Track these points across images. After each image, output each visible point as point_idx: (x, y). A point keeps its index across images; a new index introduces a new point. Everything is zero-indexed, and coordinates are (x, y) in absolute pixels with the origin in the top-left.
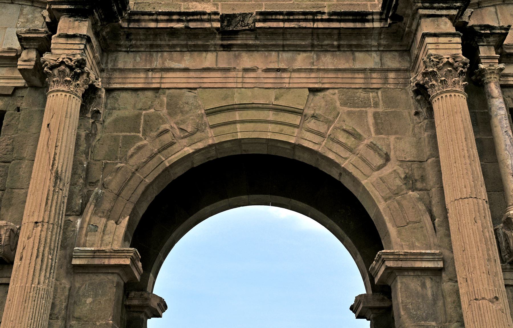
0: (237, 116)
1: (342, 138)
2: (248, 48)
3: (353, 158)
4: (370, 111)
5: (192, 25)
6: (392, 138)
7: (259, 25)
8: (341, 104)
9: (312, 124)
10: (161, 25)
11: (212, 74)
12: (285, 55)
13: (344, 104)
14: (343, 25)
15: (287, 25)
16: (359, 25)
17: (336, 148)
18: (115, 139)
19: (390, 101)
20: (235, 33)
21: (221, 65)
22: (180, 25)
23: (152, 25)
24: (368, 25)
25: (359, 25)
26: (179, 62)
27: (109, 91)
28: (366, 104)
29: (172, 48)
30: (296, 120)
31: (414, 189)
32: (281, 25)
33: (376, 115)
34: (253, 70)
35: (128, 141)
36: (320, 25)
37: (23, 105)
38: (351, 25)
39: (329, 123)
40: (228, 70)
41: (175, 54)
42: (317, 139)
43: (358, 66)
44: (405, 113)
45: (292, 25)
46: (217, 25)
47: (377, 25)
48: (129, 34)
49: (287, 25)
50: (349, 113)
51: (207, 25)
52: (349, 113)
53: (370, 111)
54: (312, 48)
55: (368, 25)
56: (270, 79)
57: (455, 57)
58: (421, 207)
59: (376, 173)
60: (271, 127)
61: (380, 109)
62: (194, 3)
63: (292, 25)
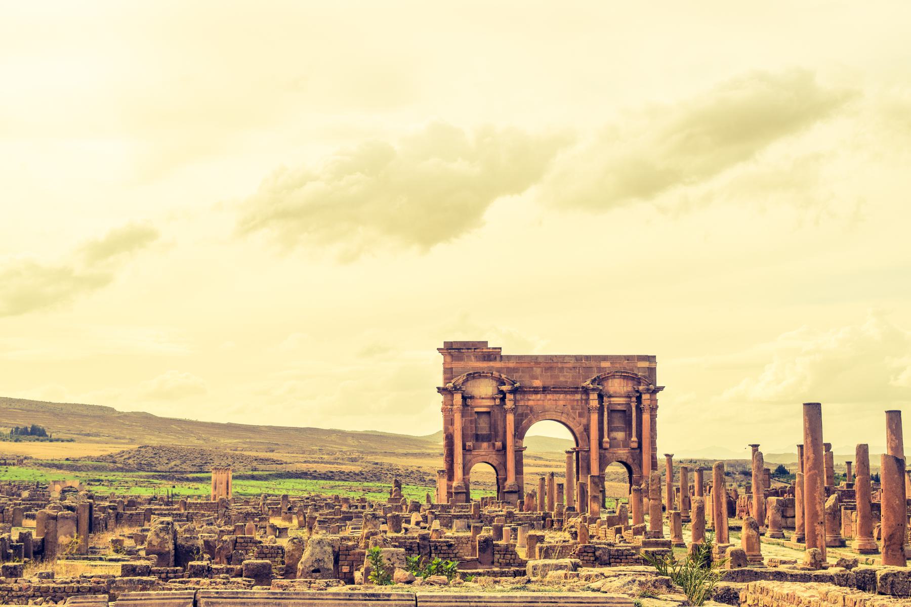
0: (547, 413)
1: (571, 419)
2: (548, 393)
3: (572, 424)
4: (578, 411)
5: (535, 390)
6: (582, 419)
7: (552, 390)
8: (571, 409)
9: (564, 415)
10: (528, 390)
11: (540, 401)
12: (558, 395)
13: (571, 409)
14: (572, 390)
15: (559, 390)
16: (576, 390)
17: (569, 421)
18: (518, 419)
19: (582, 409)
20: (546, 391)
21: (542, 399)
22: (533, 390)
23: (526, 390)
24: (578, 390)
25: (576, 390)
26: (532, 397)
27: (515, 406)
28: (577, 409)
29: (529, 393)
30: (560, 414)
31: (586, 432)
32: (557, 390)
33: (579, 413)
34: (550, 400)
35: (522, 420)
36: (567, 390)
37: (495, 410)
38: (574, 390)
39: (568, 415)
40: (544, 400)
41: (531, 395)
42: (565, 419)
43: (576, 398)
44: (586, 412)
45: (560, 390)
46: (542, 390)
47: (581, 390)
48: (519, 391)
49: (559, 390)
50: (573, 412)
51: (539, 390)
52: (573, 412)
53: (578, 411)
54: (564, 393)
55: (578, 390)
56: (554, 403)
57: (596, 406)
58: (586, 436)
59: (578, 428)
60: (554, 416)
61: (580, 411)
62: (535, 380)
63: (560, 390)
